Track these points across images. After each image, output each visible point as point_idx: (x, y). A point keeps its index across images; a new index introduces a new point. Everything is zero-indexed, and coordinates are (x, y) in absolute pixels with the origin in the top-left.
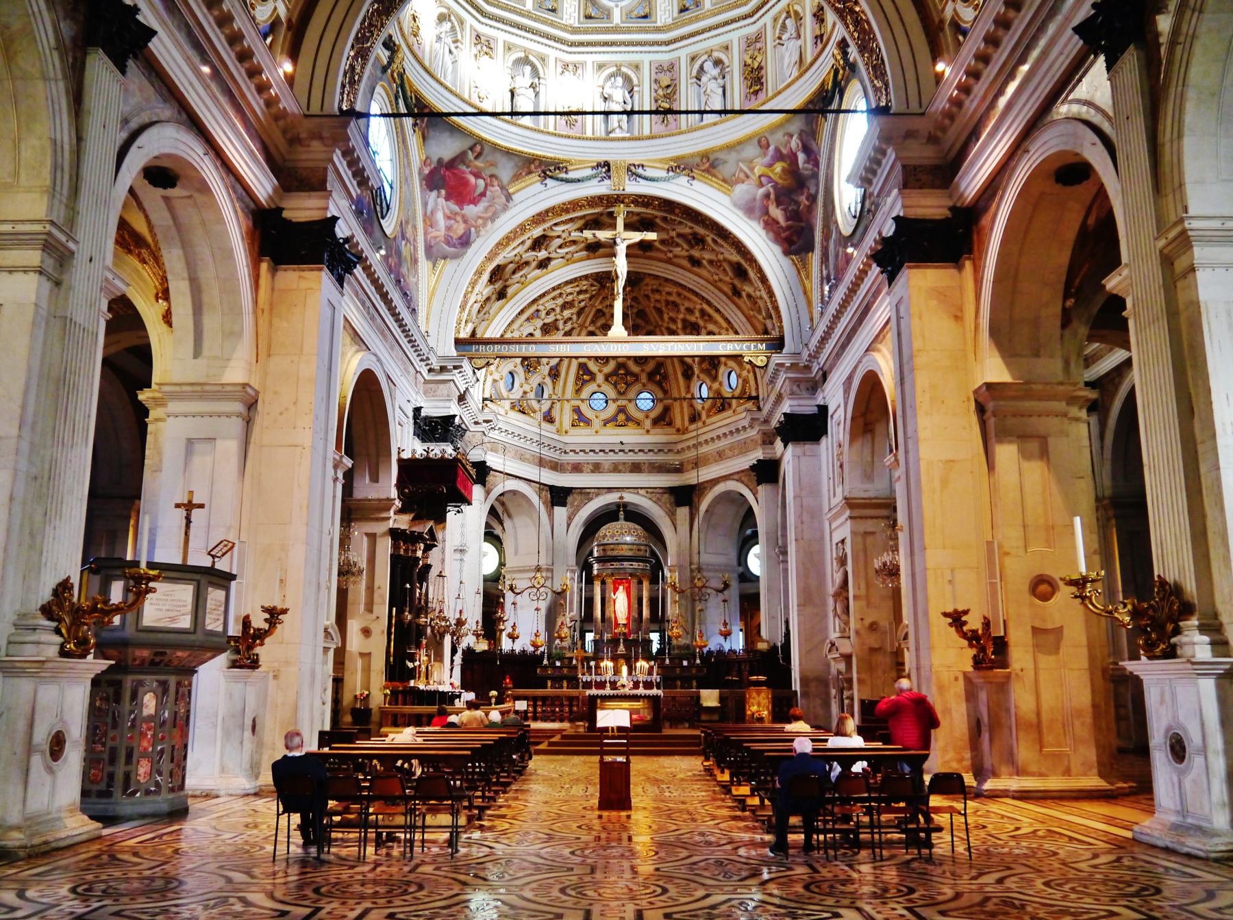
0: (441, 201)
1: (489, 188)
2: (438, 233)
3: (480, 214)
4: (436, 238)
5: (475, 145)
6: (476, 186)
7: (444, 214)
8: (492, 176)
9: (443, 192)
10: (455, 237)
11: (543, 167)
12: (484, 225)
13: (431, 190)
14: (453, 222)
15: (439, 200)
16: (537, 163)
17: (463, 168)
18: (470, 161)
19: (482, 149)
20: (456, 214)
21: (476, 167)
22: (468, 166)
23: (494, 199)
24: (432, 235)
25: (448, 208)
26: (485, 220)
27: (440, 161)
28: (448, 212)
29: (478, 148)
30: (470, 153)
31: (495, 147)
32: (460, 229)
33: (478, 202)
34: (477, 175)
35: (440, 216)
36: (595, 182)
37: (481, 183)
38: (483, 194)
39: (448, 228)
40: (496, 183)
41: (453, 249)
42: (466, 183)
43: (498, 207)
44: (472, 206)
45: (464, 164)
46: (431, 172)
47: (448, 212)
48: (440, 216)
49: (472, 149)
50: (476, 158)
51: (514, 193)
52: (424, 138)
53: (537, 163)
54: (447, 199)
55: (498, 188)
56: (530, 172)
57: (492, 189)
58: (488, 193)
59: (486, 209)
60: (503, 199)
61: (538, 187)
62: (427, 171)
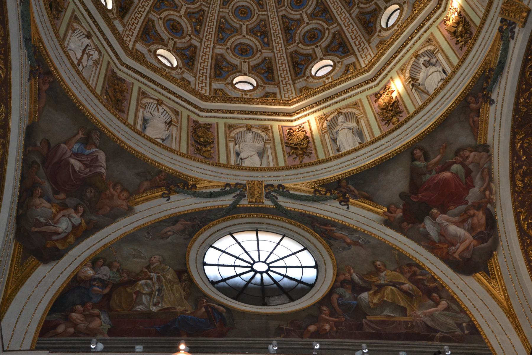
0: (441, 218)
1: (467, 163)
2: (467, 243)
3: (482, 189)
4: (467, 248)
5: (412, 154)
6: (456, 174)
7: (456, 224)
8: (457, 153)
9: (435, 211)
10: (483, 228)
11: (480, 94)
12: (491, 191)
13: (422, 221)
14: (469, 221)
15: (438, 219)
16: (471, 99)
17: (428, 176)
18: (427, 167)
19: (422, 149)
20: (466, 211)
21: (436, 164)
22: (430, 172)
23: (479, 164)
24: (460, 250)
25: (454, 216)
26: (489, 188)
27: (402, 196)
28: (457, 219)
29: (418, 153)
30: (417, 163)
31: (428, 135)
32: (481, 217)
33: (472, 182)
34: (447, 168)
35: (453, 229)
36: (512, 42)
37: (456, 167)
38: (468, 172)
39: (471, 230)
40: (467, 153)
41: (490, 240)
42: (446, 182)
43: (486, 166)
44: (472, 191)
45: (425, 174)
46: (404, 211)
47: (457, 219)
48: (453, 229)
49: (414, 159)
50: (427, 158)
51: (486, 140)
52: (368, 198)
53: (471, 99)
54: (444, 211)
55: (473, 154)
56: (478, 111)
57: (470, 159)
58: (471, 167)
59: (483, 179)
60: (484, 154)
61: (492, 108)
62: (399, 214)
